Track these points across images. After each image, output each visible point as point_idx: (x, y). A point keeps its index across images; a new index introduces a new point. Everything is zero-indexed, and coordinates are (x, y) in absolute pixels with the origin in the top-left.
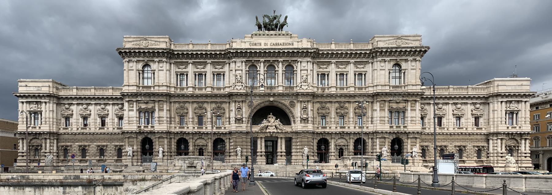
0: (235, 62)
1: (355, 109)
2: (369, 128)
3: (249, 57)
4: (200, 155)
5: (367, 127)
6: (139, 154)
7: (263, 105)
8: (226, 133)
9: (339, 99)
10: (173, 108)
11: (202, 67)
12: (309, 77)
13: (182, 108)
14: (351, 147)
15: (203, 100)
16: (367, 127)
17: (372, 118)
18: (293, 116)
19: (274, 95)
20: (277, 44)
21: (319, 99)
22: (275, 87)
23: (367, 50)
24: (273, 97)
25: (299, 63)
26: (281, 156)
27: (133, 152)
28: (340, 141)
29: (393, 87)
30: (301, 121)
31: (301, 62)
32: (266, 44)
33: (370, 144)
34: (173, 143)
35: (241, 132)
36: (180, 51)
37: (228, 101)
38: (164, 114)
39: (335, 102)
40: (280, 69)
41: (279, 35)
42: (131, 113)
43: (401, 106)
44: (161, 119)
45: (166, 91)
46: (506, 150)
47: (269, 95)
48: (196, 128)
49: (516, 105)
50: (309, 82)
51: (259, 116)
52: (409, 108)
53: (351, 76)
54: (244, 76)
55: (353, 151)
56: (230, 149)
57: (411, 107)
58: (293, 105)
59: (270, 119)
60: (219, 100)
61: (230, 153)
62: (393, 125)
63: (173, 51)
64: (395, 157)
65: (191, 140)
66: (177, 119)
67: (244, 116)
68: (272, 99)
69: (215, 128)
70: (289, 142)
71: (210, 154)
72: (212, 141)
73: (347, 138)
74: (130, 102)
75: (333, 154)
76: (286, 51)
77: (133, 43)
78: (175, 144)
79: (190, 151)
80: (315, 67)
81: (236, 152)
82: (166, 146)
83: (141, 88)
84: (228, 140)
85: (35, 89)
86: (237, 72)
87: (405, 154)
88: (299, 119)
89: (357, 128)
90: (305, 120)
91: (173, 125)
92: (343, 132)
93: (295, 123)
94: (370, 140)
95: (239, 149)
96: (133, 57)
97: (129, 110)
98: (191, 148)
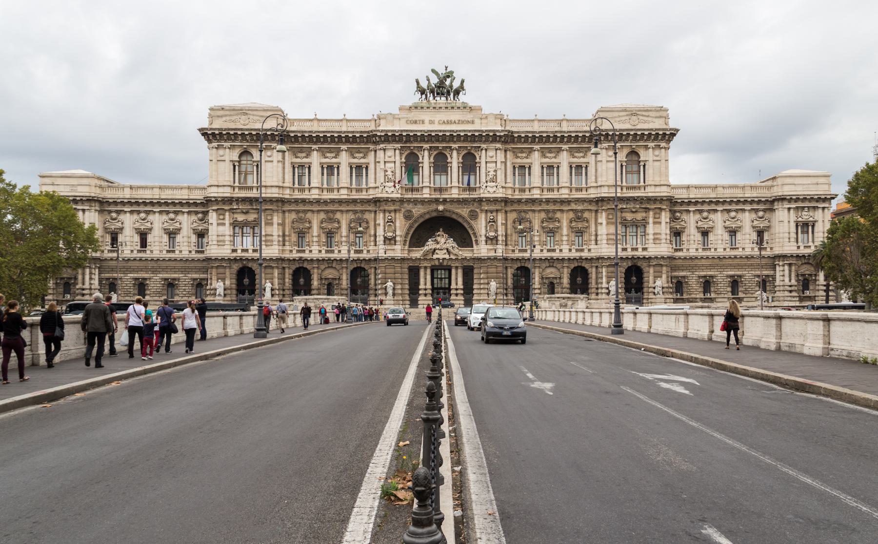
0: (385, 150)
1: (571, 222)
2: (592, 251)
3: (406, 142)
4: (329, 294)
5: (589, 250)
6: (234, 292)
7: (427, 217)
8: (370, 260)
9: (545, 207)
10: (287, 221)
11: (333, 155)
12: (499, 173)
13: (301, 220)
14: (566, 281)
15: (335, 207)
16: (589, 250)
17: (596, 235)
18: (475, 234)
19: (445, 200)
20: (449, 122)
21: (516, 207)
22: (446, 189)
23: (586, 132)
24: (444, 204)
25: (484, 151)
26: (457, 295)
27: (225, 290)
28: (549, 270)
29: (628, 188)
30: (486, 242)
31: (486, 150)
32: (432, 122)
33: (594, 276)
34: (287, 276)
35: (393, 259)
36: (299, 132)
37: (374, 209)
38: (275, 231)
39: (540, 211)
40: (455, 160)
41: (453, 108)
42: (221, 228)
43: (639, 216)
44: (268, 238)
45: (277, 195)
46: (798, 281)
47: (437, 201)
48: (323, 252)
49: (811, 214)
50: (499, 180)
51: (422, 232)
52: (651, 220)
53: (564, 170)
54: (398, 172)
55: (568, 286)
56: (376, 285)
57: (655, 218)
58: (474, 216)
59: (439, 239)
60: (359, 208)
61: (376, 290)
62: (628, 246)
63: (288, 132)
64: (633, 294)
65: (316, 271)
66: (294, 238)
67: (398, 233)
68: (441, 208)
69: (352, 252)
70: (468, 273)
71: (345, 292)
72: (349, 271)
73: (559, 266)
74: (220, 212)
75: (537, 291)
76: (462, 134)
77: (224, 119)
78: (291, 277)
79: (313, 287)
80: (508, 156)
81: (386, 288)
82: (276, 281)
83: (237, 190)
84: (373, 270)
85: (68, 189)
86: (387, 165)
87: (645, 290)
88: (484, 238)
89: (574, 251)
90: (492, 240)
91: (288, 248)
92: (552, 258)
93: (477, 244)
94: (594, 270)
95: (390, 284)
96: (225, 141)
97: (218, 224)
98: (315, 283)
